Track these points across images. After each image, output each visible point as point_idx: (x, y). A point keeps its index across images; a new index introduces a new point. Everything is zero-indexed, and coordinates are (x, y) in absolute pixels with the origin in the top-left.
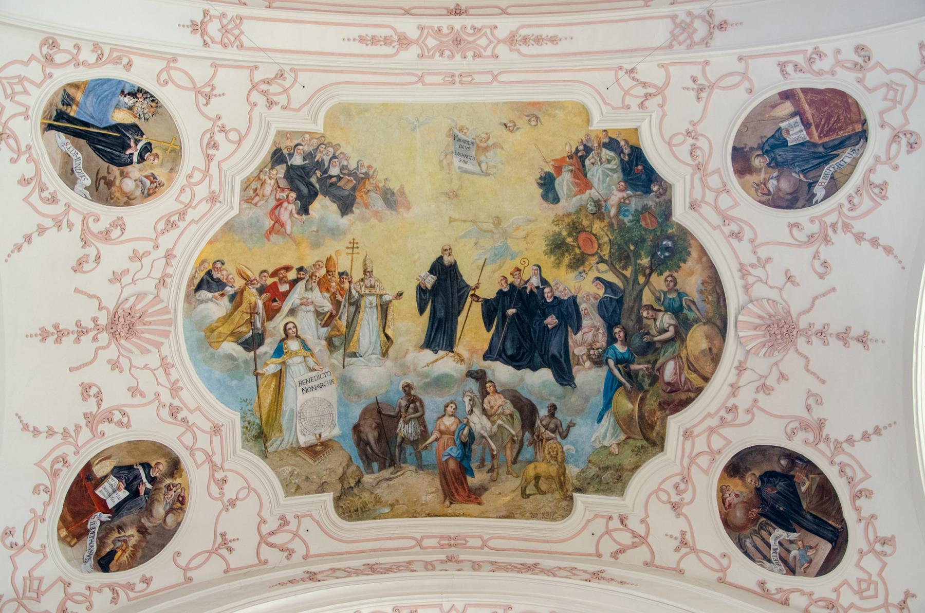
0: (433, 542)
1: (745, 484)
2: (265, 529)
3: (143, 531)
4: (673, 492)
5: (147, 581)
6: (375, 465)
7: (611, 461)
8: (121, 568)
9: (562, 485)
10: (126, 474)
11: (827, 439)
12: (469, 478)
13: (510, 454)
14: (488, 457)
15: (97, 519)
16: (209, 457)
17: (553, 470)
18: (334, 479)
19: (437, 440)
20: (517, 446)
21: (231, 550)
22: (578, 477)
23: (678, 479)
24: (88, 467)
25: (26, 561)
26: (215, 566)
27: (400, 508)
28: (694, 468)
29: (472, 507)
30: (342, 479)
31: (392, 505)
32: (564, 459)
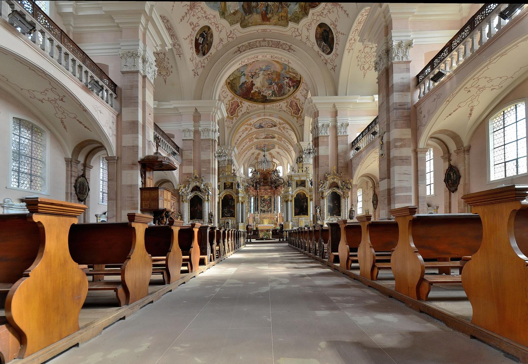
0: (260, 31)
1: (321, 30)
2: (228, 35)
3: (207, 44)
4: (308, 26)
5: (211, 54)
6: (247, 14)
7: (297, 15)
8: (207, 54)
9: (287, 19)
10: (202, 35)
11: (336, 29)
12: (267, 15)
13: (276, 10)
14: (271, 10)
15: (200, 48)
16: (214, 23)
17: (285, 15)
18: (239, 19)
19: (260, 6)
20: (278, 8)
21: (223, 41)
22: (290, 17)
23: (309, 23)
24: (196, 38)
25: (194, 61)
26: (221, 45)
27: (253, 24)
28: (313, 24)
29: (268, 23)
30: (241, 19)
31: (252, 23)
32: (287, 13)
